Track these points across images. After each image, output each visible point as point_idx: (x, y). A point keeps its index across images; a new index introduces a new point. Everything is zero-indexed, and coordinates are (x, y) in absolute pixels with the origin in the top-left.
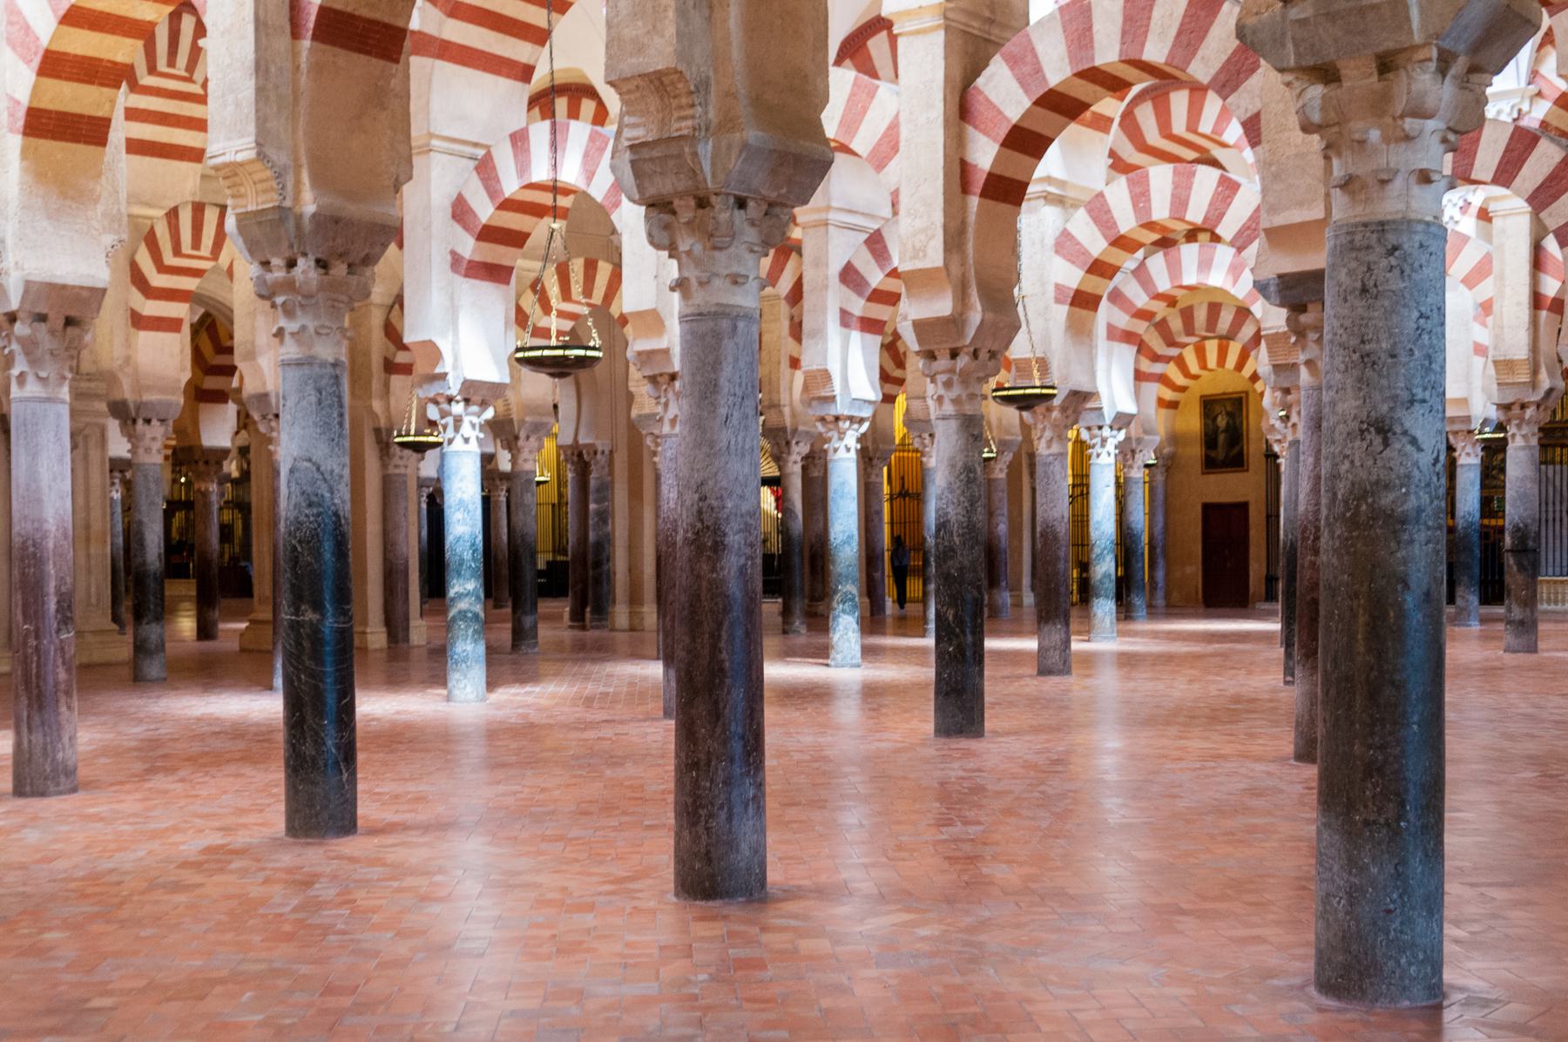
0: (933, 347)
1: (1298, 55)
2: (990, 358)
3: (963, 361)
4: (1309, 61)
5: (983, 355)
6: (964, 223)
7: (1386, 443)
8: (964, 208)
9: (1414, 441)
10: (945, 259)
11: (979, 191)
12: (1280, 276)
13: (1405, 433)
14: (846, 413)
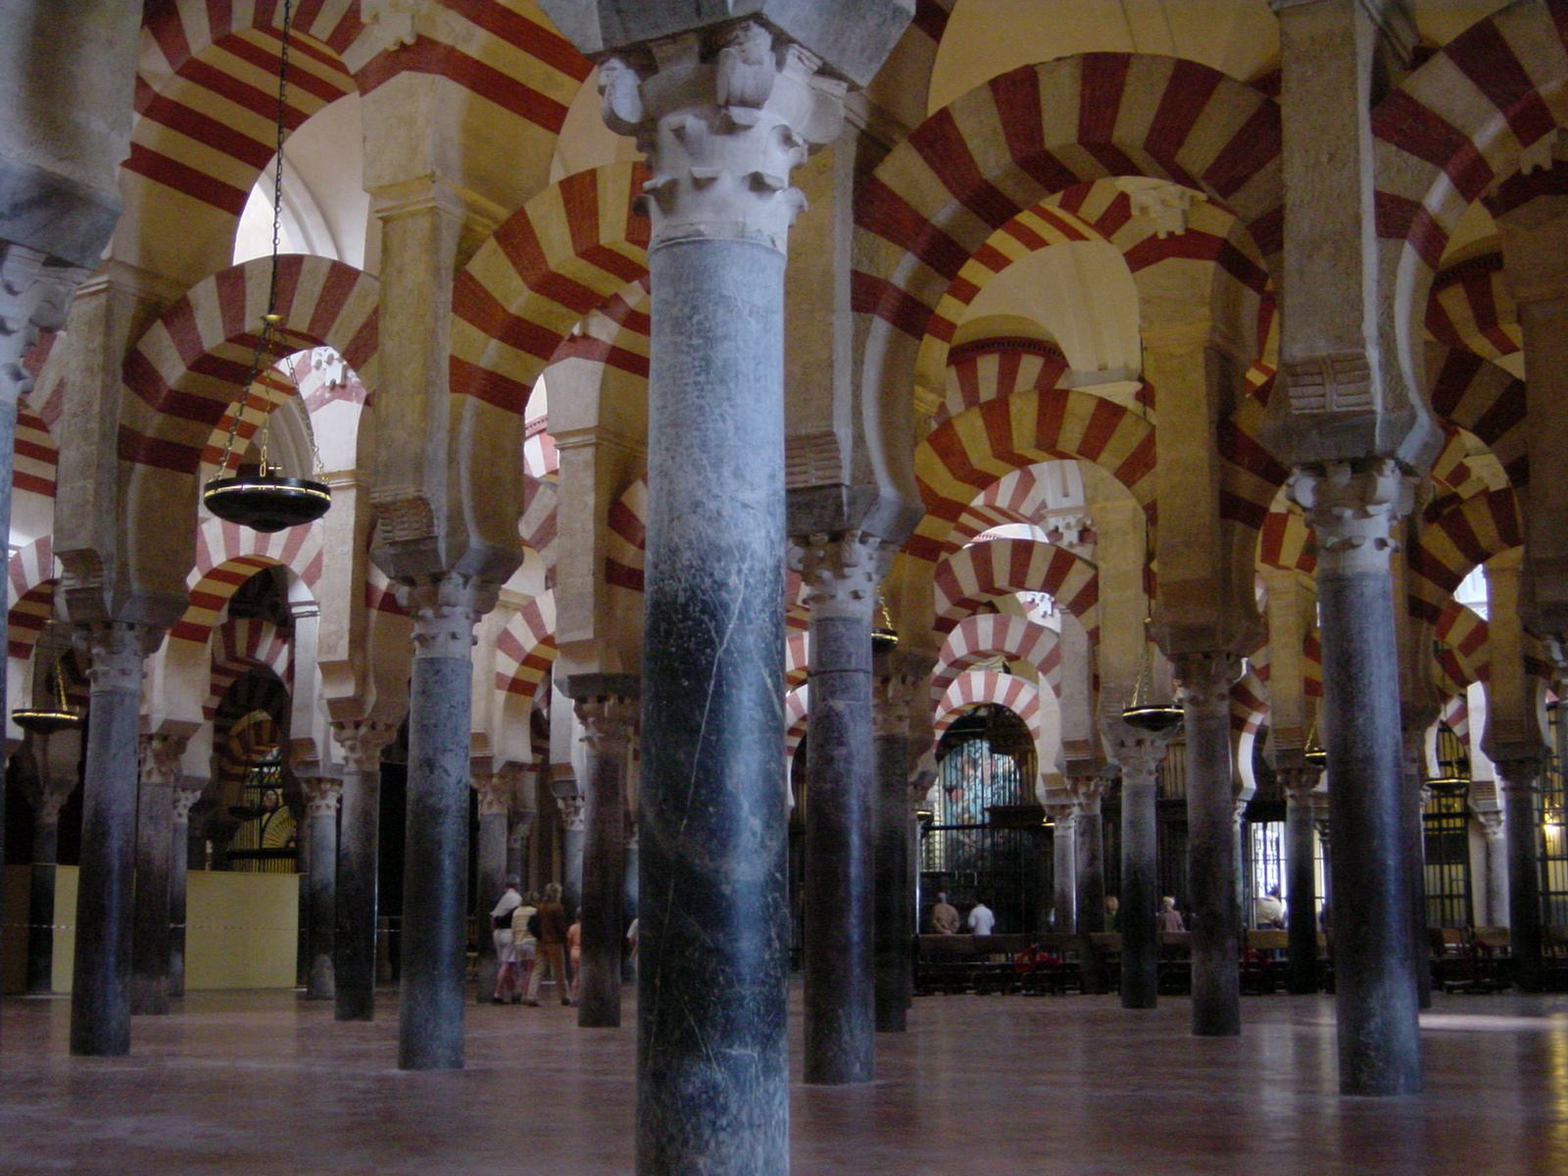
0: (342, 720)
1: (397, 572)
2: (386, 730)
3: (363, 730)
4: (400, 575)
5: (381, 726)
6: (366, 629)
7: (432, 772)
8: (367, 617)
9: (446, 771)
10: (350, 655)
11: (377, 605)
12: (570, 677)
13: (441, 767)
14: (328, 776)
